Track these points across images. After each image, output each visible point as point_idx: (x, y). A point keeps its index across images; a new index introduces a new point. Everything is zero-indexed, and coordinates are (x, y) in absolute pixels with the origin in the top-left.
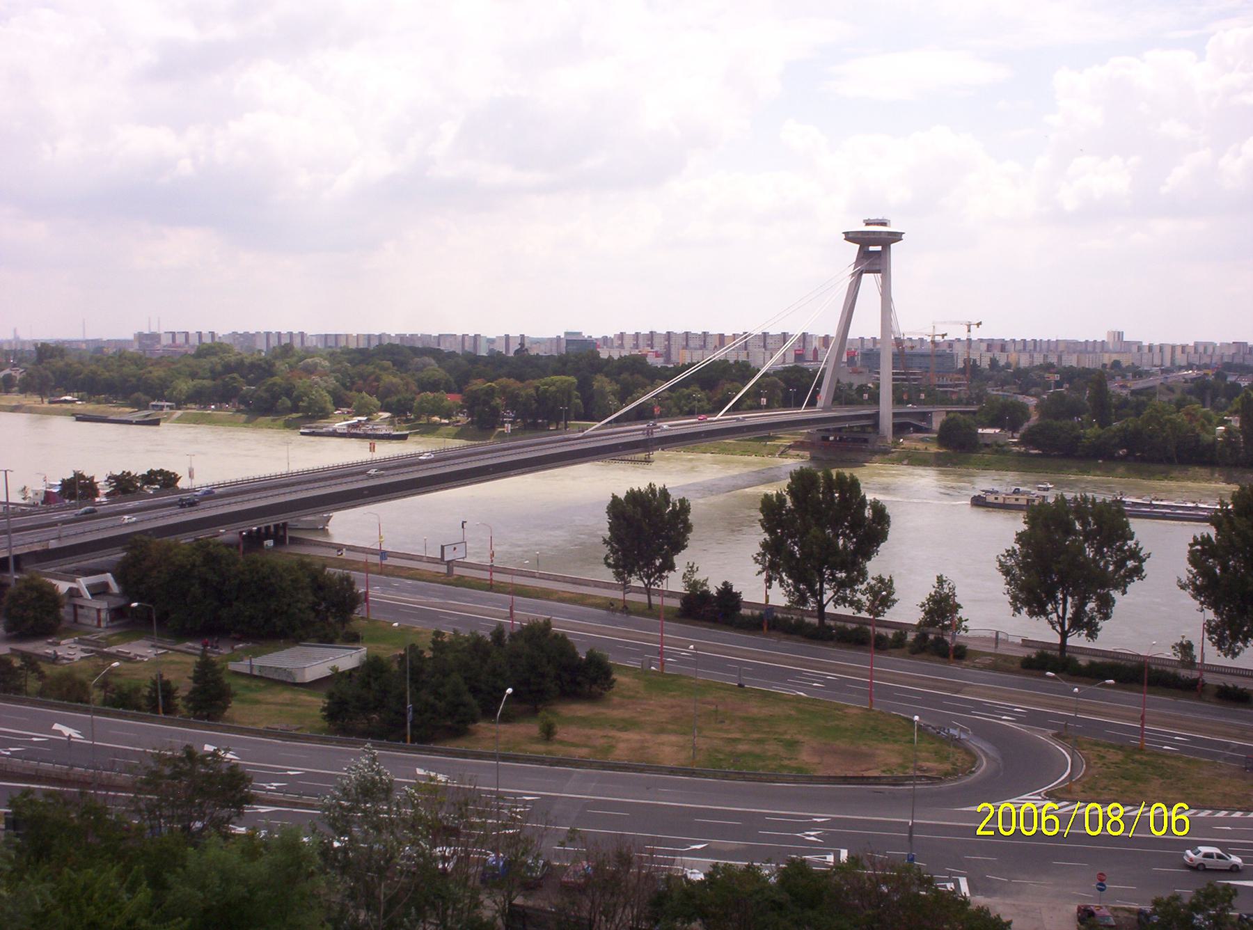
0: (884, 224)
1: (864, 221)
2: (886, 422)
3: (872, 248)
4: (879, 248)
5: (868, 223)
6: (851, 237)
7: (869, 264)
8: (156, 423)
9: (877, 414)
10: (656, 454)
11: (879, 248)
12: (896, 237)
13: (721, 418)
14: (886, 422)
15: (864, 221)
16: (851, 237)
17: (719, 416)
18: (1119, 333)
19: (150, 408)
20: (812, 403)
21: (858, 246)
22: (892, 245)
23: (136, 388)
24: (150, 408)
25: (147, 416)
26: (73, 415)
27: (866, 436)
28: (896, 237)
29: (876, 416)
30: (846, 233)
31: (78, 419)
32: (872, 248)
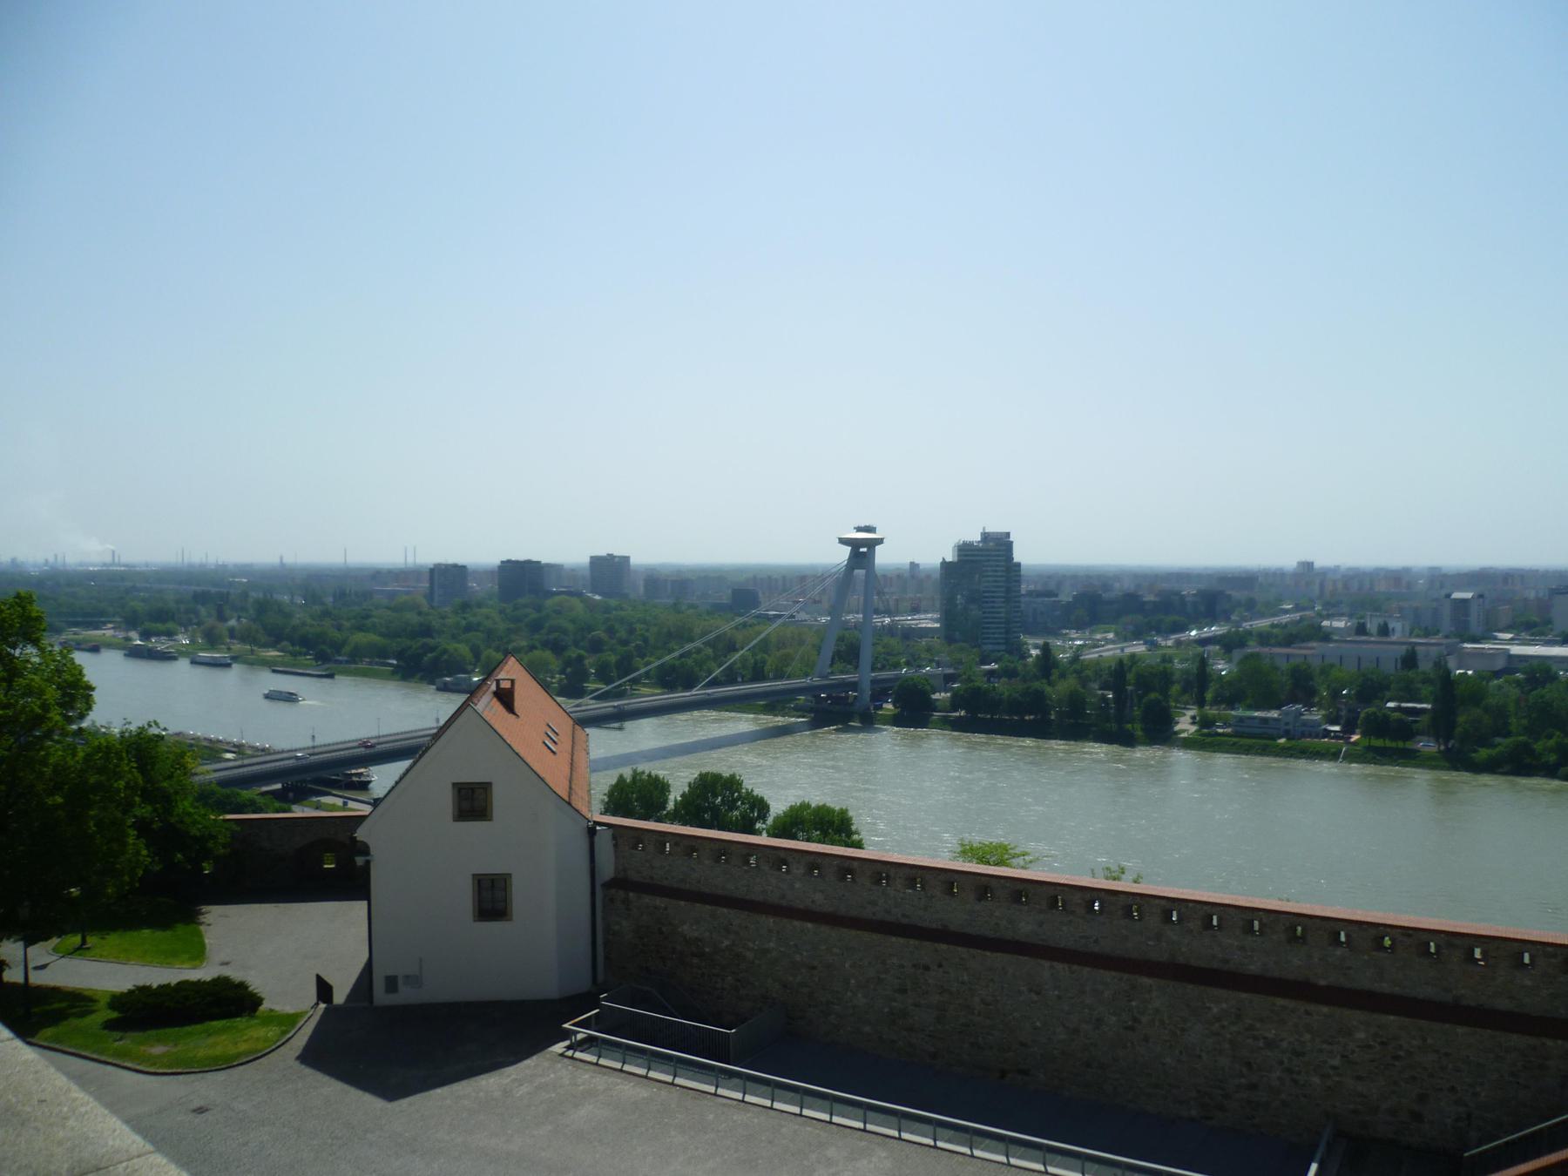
1: (855, 528)
3: (861, 550)
4: (864, 550)
5: (859, 529)
6: (843, 541)
8: (331, 676)
10: (628, 725)
11: (864, 550)
12: (880, 541)
13: (696, 693)
15: (855, 528)
16: (843, 541)
17: (694, 692)
21: (850, 548)
22: (877, 547)
28: (880, 541)
30: (840, 539)
31: (274, 671)
32: (861, 550)
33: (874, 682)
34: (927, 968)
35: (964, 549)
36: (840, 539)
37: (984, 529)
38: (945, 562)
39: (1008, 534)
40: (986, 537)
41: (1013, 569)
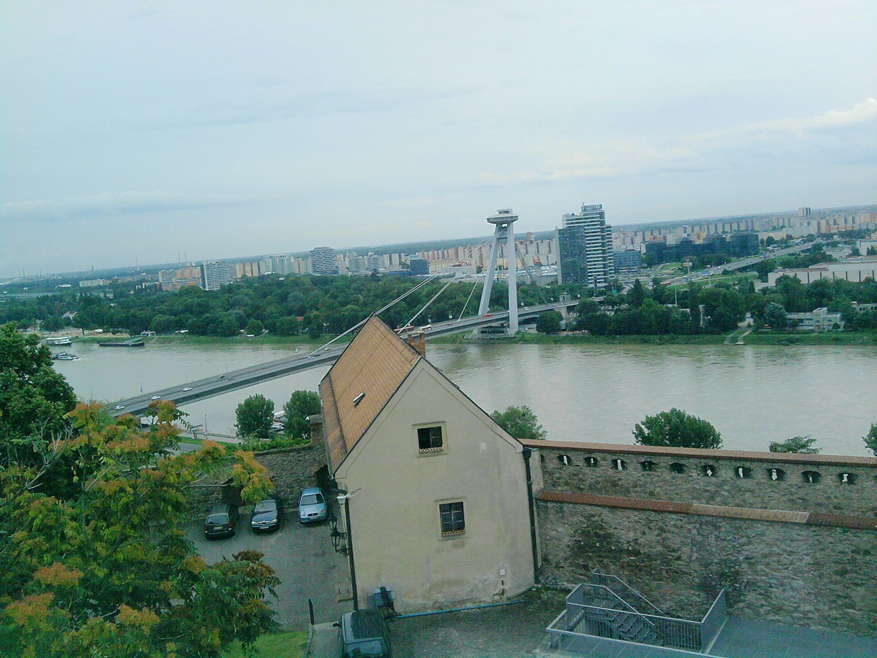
0: (507, 212)
1: (498, 211)
2: (514, 320)
3: (503, 225)
4: (506, 225)
7: (502, 234)
8: (142, 345)
9: (508, 317)
11: (506, 225)
12: (515, 219)
14: (514, 320)
15: (498, 211)
18: (807, 209)
19: (142, 335)
20: (476, 310)
23: (134, 323)
24: (142, 335)
25: (139, 341)
26: (98, 343)
27: (501, 329)
28: (515, 219)
29: (507, 319)
31: (101, 345)
32: (503, 225)
33: (519, 316)
34: (867, 553)
35: (571, 219)
36: (488, 219)
37: (583, 204)
38: (560, 230)
39: (601, 205)
40: (585, 209)
41: (605, 231)
